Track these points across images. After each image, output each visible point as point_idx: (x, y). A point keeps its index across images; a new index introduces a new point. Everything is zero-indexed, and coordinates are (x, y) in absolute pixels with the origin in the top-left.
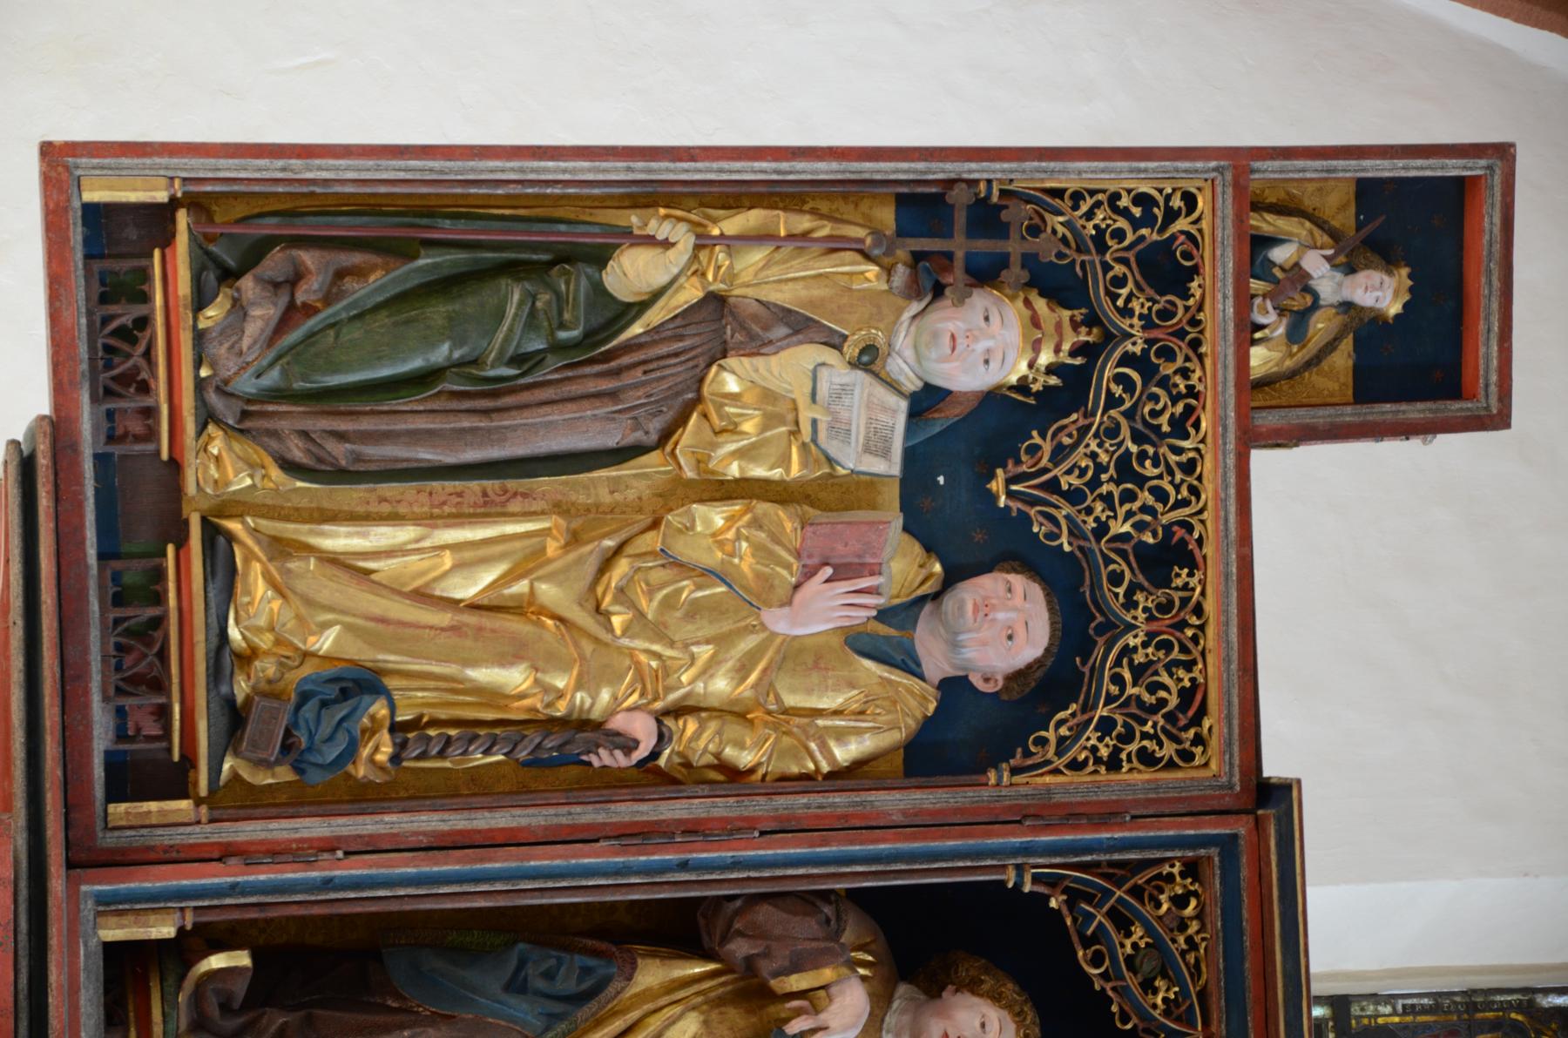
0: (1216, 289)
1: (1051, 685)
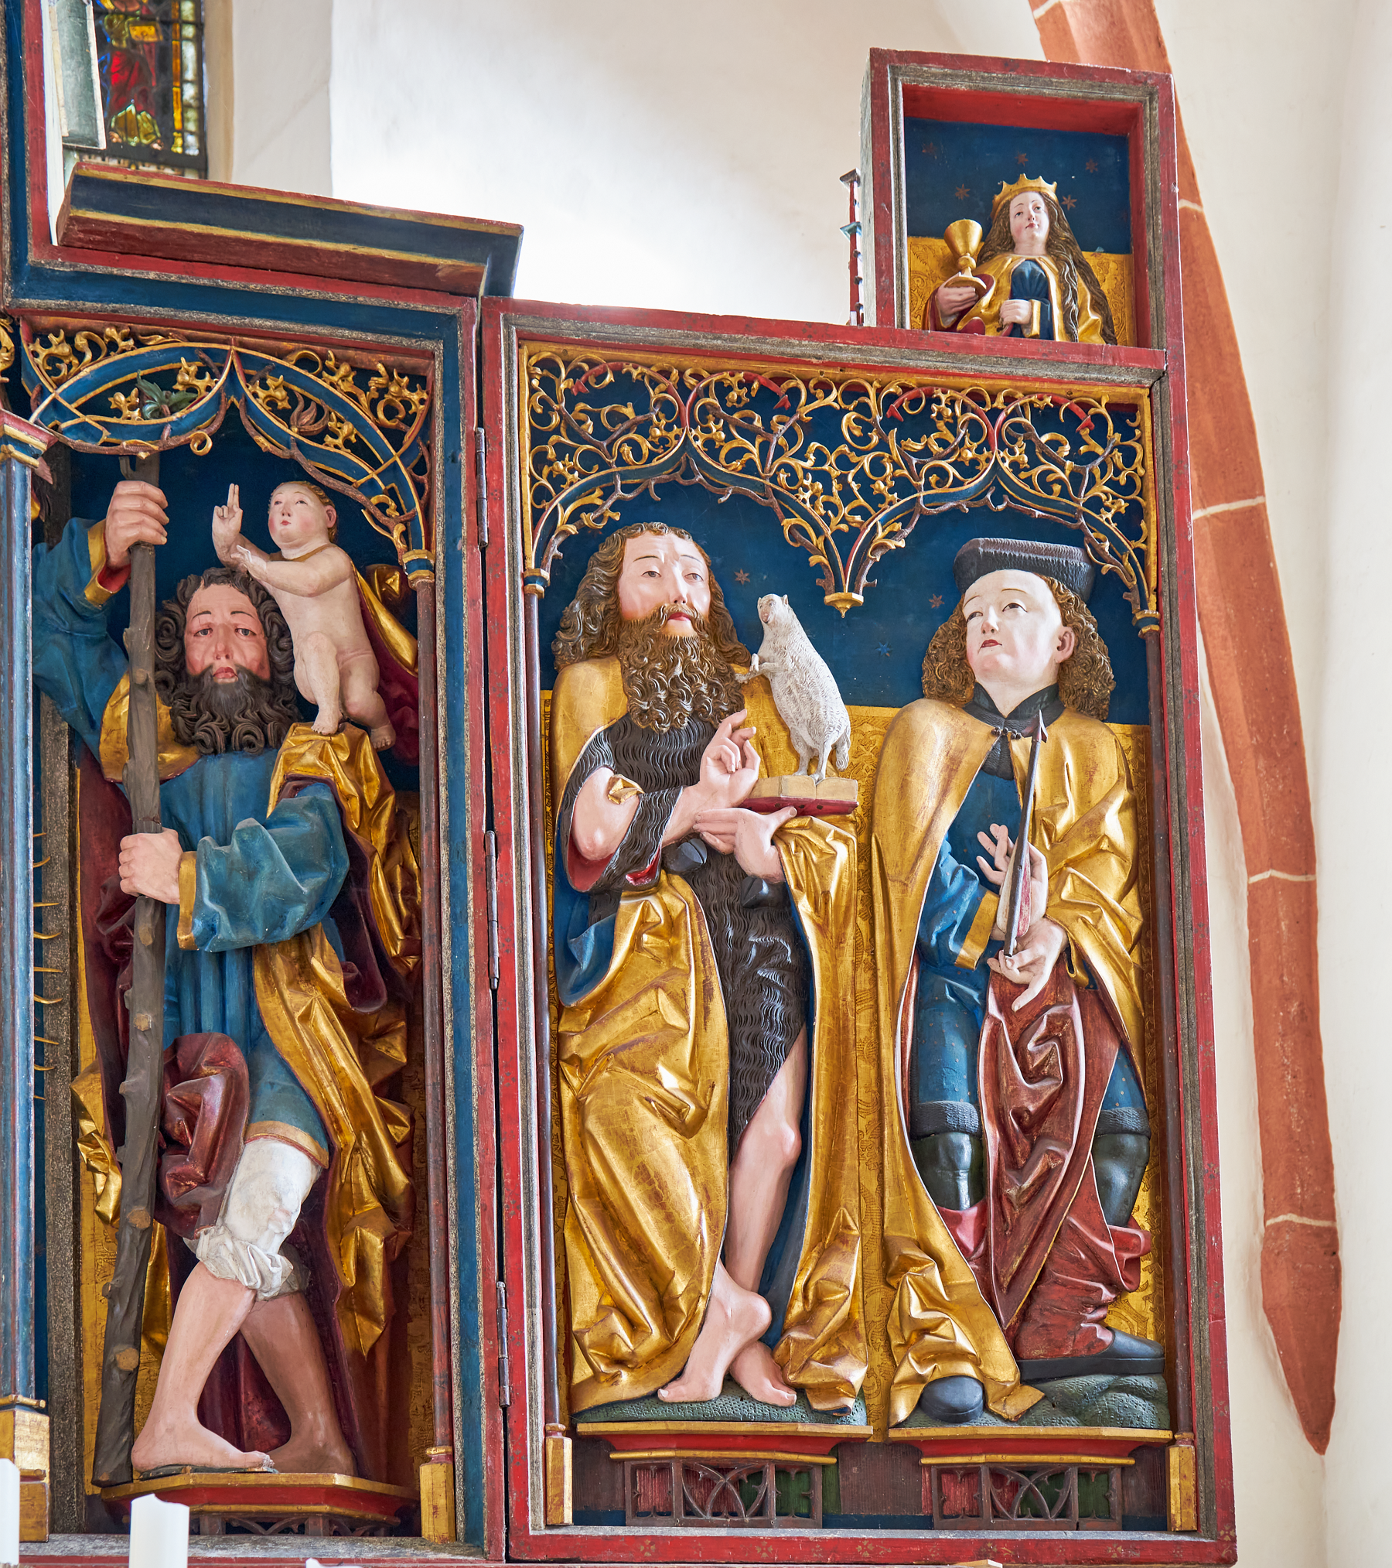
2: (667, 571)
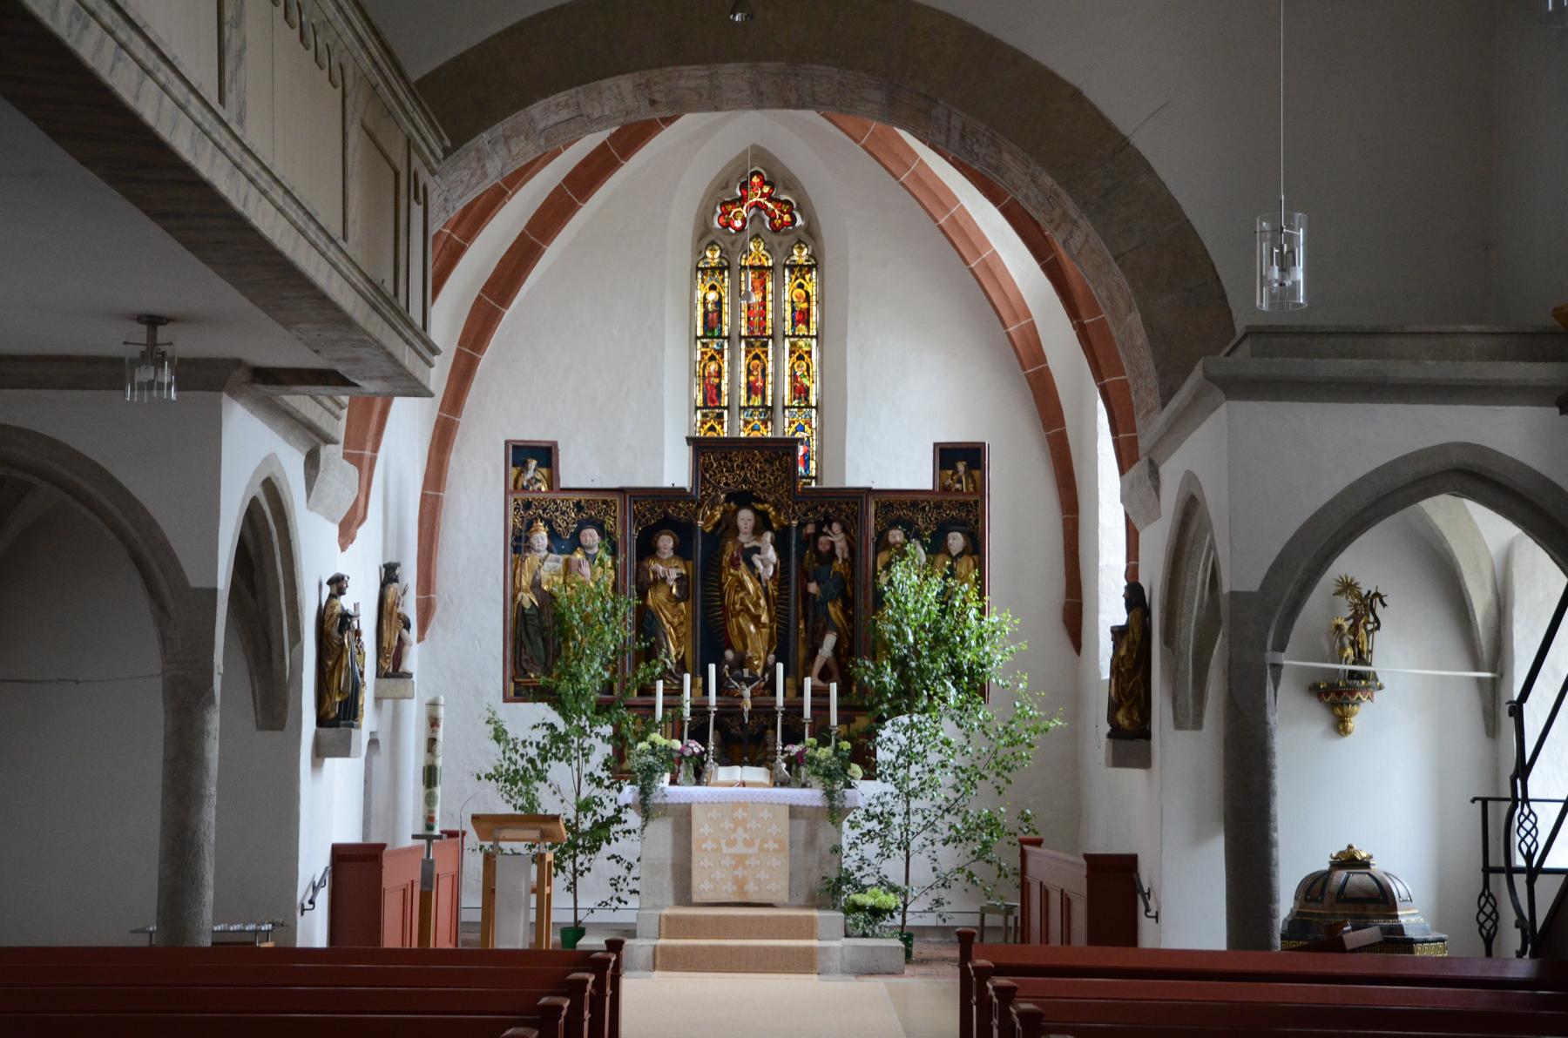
0: (530, 497)
2: (896, 535)
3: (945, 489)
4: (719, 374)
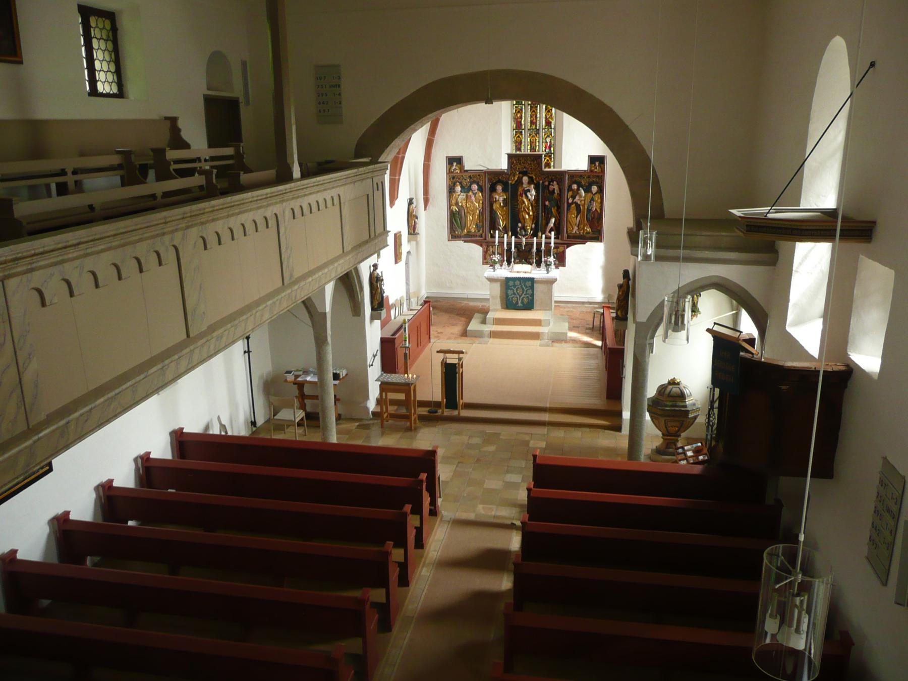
1: (478, 185)
2: (575, 187)
3: (591, 171)
4: (521, 117)
